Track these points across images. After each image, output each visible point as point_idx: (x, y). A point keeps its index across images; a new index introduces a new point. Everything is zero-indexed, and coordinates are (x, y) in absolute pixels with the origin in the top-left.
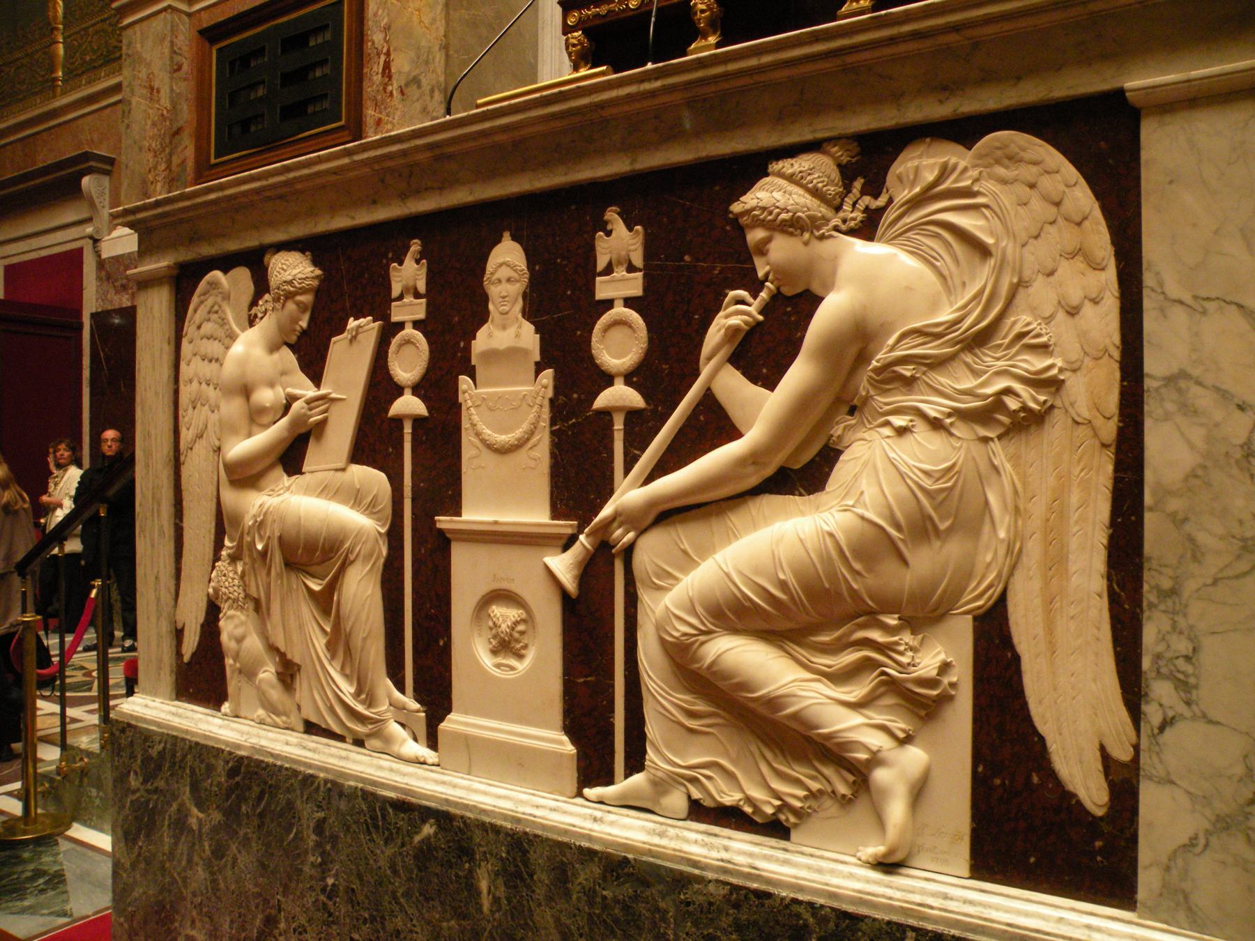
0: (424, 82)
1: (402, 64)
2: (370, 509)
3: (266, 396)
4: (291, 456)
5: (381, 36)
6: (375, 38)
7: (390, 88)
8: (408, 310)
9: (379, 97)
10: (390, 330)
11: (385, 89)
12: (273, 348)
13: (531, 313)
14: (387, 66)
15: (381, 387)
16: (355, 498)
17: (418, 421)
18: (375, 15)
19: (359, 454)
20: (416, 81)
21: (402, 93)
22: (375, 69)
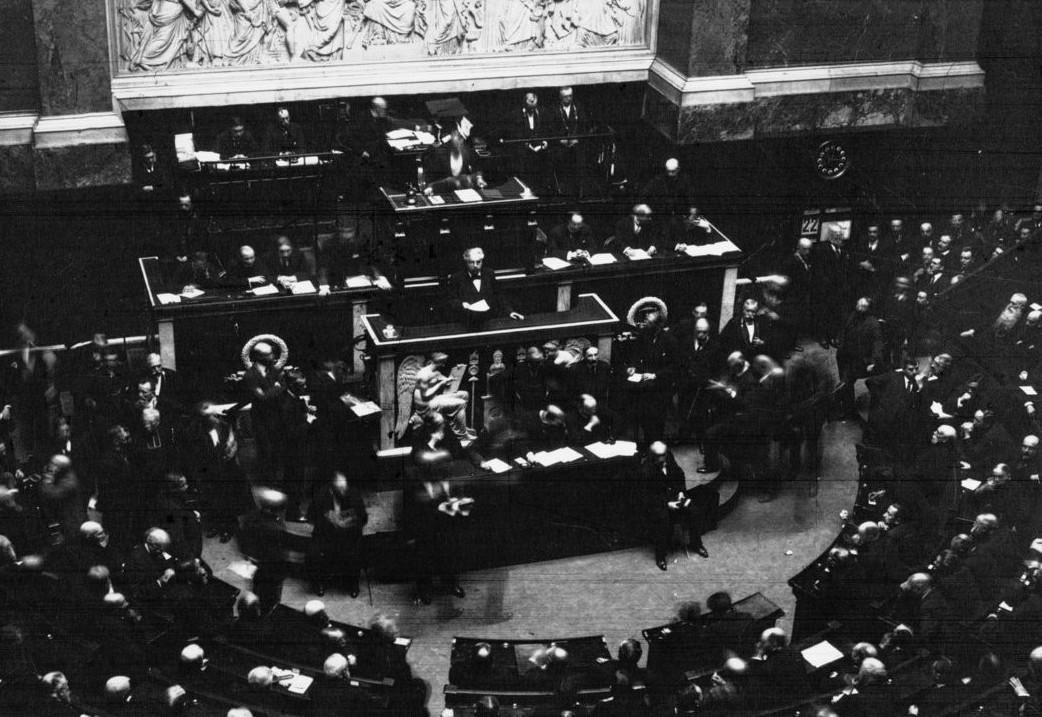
0: (92, 73)
1: (72, 59)
2: (464, 399)
3: (433, 381)
4: (440, 392)
5: (48, 38)
6: (41, 37)
7: (60, 73)
8: (474, 363)
9: (51, 77)
10: (469, 366)
11: (56, 74)
12: (434, 371)
13: (503, 361)
14: (56, 59)
15: (467, 375)
16: (461, 397)
17: (476, 382)
18: (40, 22)
19: (460, 388)
20: (85, 72)
21: (72, 77)
22: (44, 57)
